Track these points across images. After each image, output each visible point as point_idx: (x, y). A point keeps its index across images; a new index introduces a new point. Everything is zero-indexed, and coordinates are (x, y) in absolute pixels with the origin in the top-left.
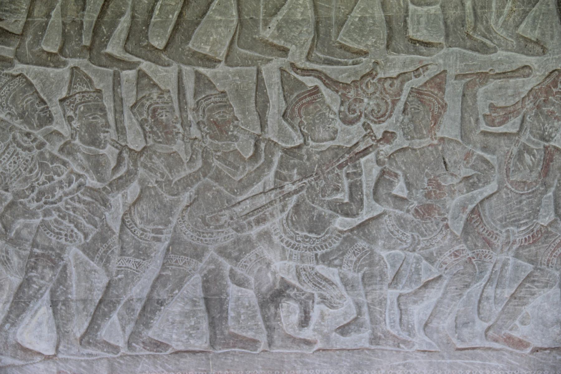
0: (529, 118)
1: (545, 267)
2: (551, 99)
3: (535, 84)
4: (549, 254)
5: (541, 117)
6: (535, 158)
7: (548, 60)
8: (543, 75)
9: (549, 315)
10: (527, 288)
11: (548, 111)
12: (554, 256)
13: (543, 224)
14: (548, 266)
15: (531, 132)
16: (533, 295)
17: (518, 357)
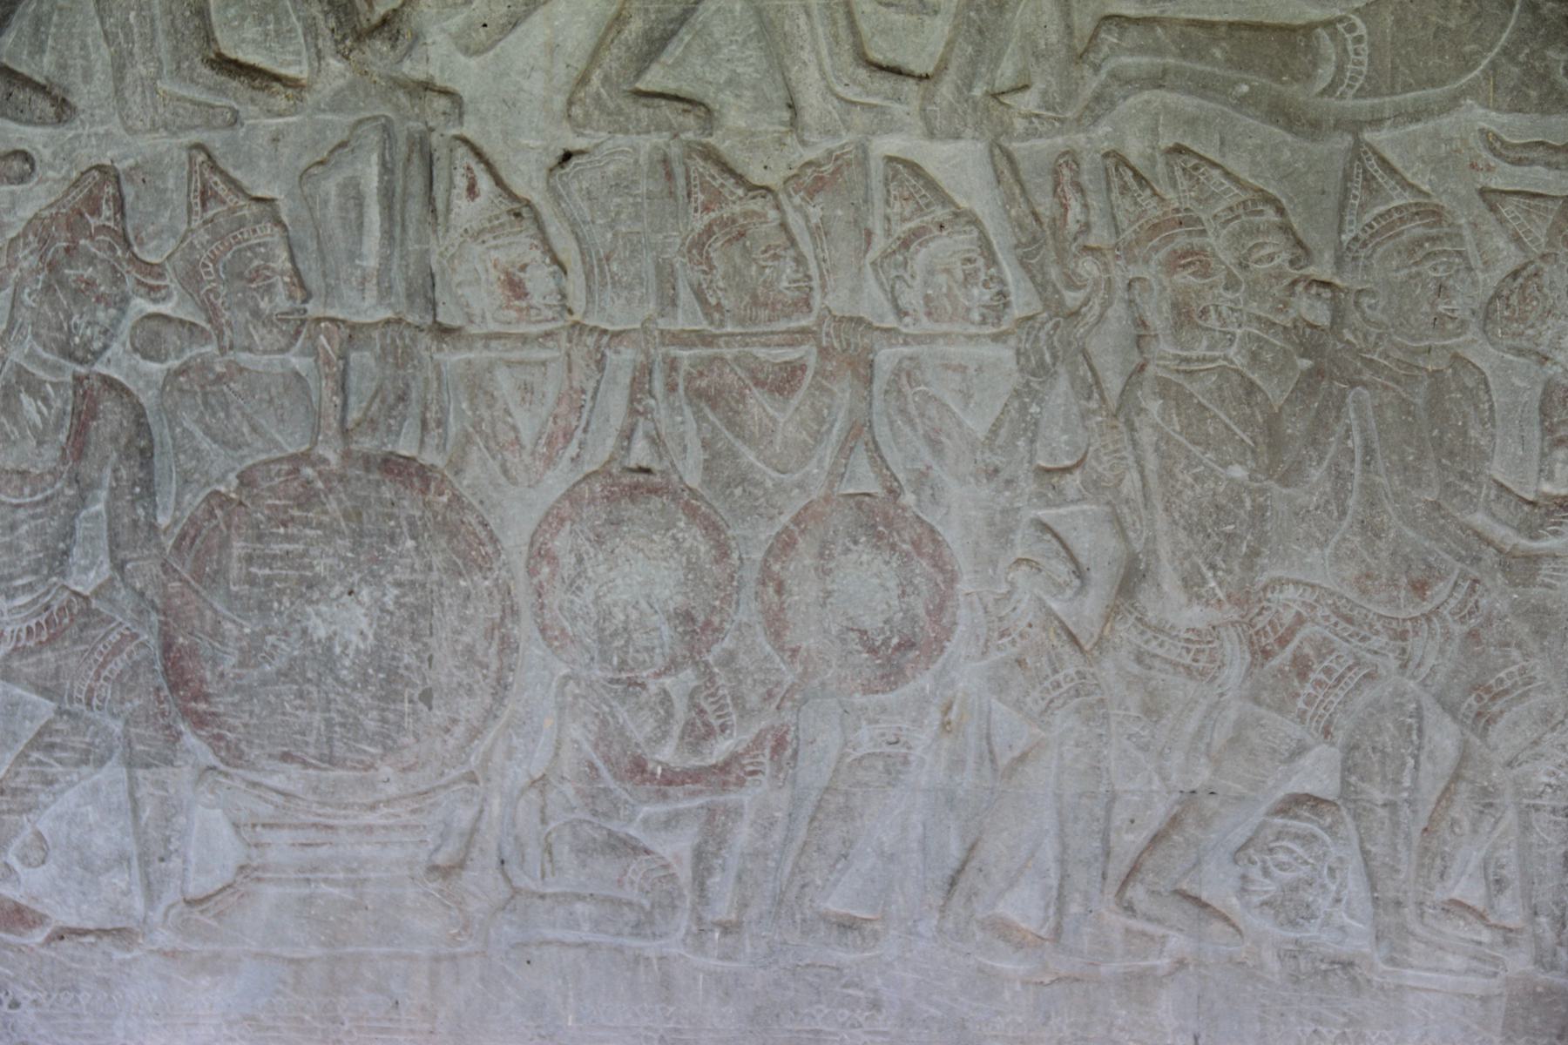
0: (30, 295)
1: (83, 707)
2: (85, 247)
3: (44, 203)
4: (91, 673)
5: (60, 294)
6: (49, 407)
7: (77, 137)
8: (64, 179)
9: (99, 840)
10: (33, 764)
11: (79, 278)
12: (106, 679)
13: (79, 589)
14: (89, 704)
15: (36, 336)
16: (51, 783)
17: (10, 954)
